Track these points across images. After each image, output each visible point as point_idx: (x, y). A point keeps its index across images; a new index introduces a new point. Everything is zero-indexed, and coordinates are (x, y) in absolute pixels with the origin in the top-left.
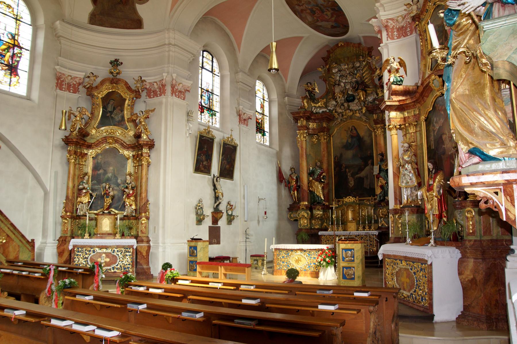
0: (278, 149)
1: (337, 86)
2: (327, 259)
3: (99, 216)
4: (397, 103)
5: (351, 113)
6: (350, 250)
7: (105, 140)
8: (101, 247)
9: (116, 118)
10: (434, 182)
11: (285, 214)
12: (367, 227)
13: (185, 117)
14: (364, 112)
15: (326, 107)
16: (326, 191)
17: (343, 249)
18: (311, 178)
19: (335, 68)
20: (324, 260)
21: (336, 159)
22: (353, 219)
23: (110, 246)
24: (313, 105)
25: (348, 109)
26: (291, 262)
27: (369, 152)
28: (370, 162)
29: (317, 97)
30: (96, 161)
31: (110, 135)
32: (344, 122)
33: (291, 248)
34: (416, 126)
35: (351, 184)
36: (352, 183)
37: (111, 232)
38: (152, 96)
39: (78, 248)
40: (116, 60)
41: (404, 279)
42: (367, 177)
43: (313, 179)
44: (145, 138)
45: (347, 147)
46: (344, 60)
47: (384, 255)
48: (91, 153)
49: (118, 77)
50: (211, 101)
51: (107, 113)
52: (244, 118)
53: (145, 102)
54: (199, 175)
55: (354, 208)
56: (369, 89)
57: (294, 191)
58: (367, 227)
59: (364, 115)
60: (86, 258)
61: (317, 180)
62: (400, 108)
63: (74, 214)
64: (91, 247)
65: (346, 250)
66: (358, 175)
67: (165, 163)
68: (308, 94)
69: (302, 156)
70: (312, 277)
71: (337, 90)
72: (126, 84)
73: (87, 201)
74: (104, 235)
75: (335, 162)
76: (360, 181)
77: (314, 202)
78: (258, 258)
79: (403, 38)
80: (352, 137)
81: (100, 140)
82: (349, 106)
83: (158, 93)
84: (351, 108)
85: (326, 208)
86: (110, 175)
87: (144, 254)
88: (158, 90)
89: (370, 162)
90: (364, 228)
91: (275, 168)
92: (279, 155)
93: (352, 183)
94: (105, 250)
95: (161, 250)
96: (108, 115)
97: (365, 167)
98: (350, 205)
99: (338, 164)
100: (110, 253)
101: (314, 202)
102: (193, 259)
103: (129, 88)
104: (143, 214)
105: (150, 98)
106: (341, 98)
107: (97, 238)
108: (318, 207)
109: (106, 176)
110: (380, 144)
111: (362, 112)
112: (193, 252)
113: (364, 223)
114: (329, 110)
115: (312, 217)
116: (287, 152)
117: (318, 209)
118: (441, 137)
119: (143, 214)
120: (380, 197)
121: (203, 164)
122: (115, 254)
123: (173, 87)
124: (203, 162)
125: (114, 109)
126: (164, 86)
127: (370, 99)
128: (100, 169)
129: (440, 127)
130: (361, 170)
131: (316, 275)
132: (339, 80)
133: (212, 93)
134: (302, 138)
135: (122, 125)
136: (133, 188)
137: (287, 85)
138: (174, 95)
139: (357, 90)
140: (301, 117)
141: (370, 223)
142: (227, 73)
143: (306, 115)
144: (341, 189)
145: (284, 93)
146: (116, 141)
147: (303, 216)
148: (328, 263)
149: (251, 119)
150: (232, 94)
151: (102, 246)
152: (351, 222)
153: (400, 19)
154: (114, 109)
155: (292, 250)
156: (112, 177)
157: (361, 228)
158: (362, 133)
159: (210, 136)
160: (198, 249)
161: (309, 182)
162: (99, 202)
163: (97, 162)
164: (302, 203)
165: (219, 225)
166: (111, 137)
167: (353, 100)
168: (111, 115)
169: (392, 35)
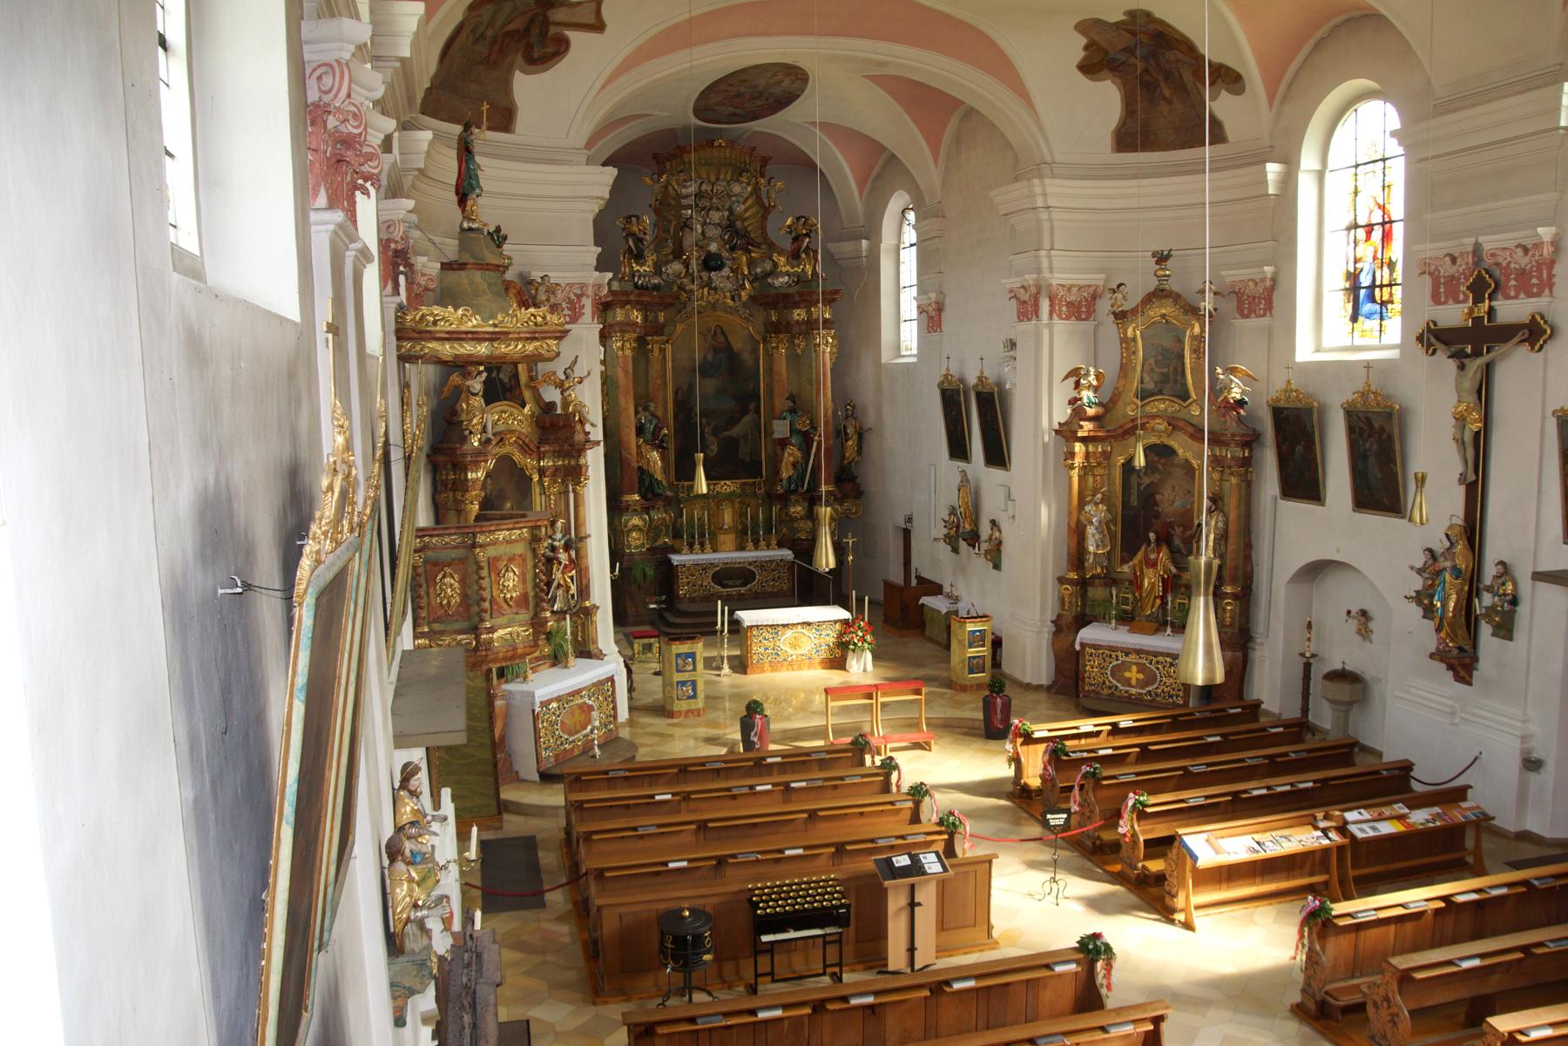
2: (868, 638)
14: (744, 298)
20: (863, 639)
22: (733, 529)
28: (752, 406)
41: (1133, 674)
45: (706, 370)
47: (1082, 645)
55: (733, 502)
59: (744, 304)
62: (1084, 440)
64: (558, 699)
71: (689, 240)
75: (676, 401)
80: (716, 350)
89: (752, 406)
99: (683, 406)
108: (660, 504)
118: (1153, 495)
130: (734, 421)
131: (837, 662)
140: (628, 302)
141: (768, 531)
152: (726, 532)
153: (1074, 290)
157: (750, 545)
158: (737, 345)
161: (638, 447)
167: (719, 268)
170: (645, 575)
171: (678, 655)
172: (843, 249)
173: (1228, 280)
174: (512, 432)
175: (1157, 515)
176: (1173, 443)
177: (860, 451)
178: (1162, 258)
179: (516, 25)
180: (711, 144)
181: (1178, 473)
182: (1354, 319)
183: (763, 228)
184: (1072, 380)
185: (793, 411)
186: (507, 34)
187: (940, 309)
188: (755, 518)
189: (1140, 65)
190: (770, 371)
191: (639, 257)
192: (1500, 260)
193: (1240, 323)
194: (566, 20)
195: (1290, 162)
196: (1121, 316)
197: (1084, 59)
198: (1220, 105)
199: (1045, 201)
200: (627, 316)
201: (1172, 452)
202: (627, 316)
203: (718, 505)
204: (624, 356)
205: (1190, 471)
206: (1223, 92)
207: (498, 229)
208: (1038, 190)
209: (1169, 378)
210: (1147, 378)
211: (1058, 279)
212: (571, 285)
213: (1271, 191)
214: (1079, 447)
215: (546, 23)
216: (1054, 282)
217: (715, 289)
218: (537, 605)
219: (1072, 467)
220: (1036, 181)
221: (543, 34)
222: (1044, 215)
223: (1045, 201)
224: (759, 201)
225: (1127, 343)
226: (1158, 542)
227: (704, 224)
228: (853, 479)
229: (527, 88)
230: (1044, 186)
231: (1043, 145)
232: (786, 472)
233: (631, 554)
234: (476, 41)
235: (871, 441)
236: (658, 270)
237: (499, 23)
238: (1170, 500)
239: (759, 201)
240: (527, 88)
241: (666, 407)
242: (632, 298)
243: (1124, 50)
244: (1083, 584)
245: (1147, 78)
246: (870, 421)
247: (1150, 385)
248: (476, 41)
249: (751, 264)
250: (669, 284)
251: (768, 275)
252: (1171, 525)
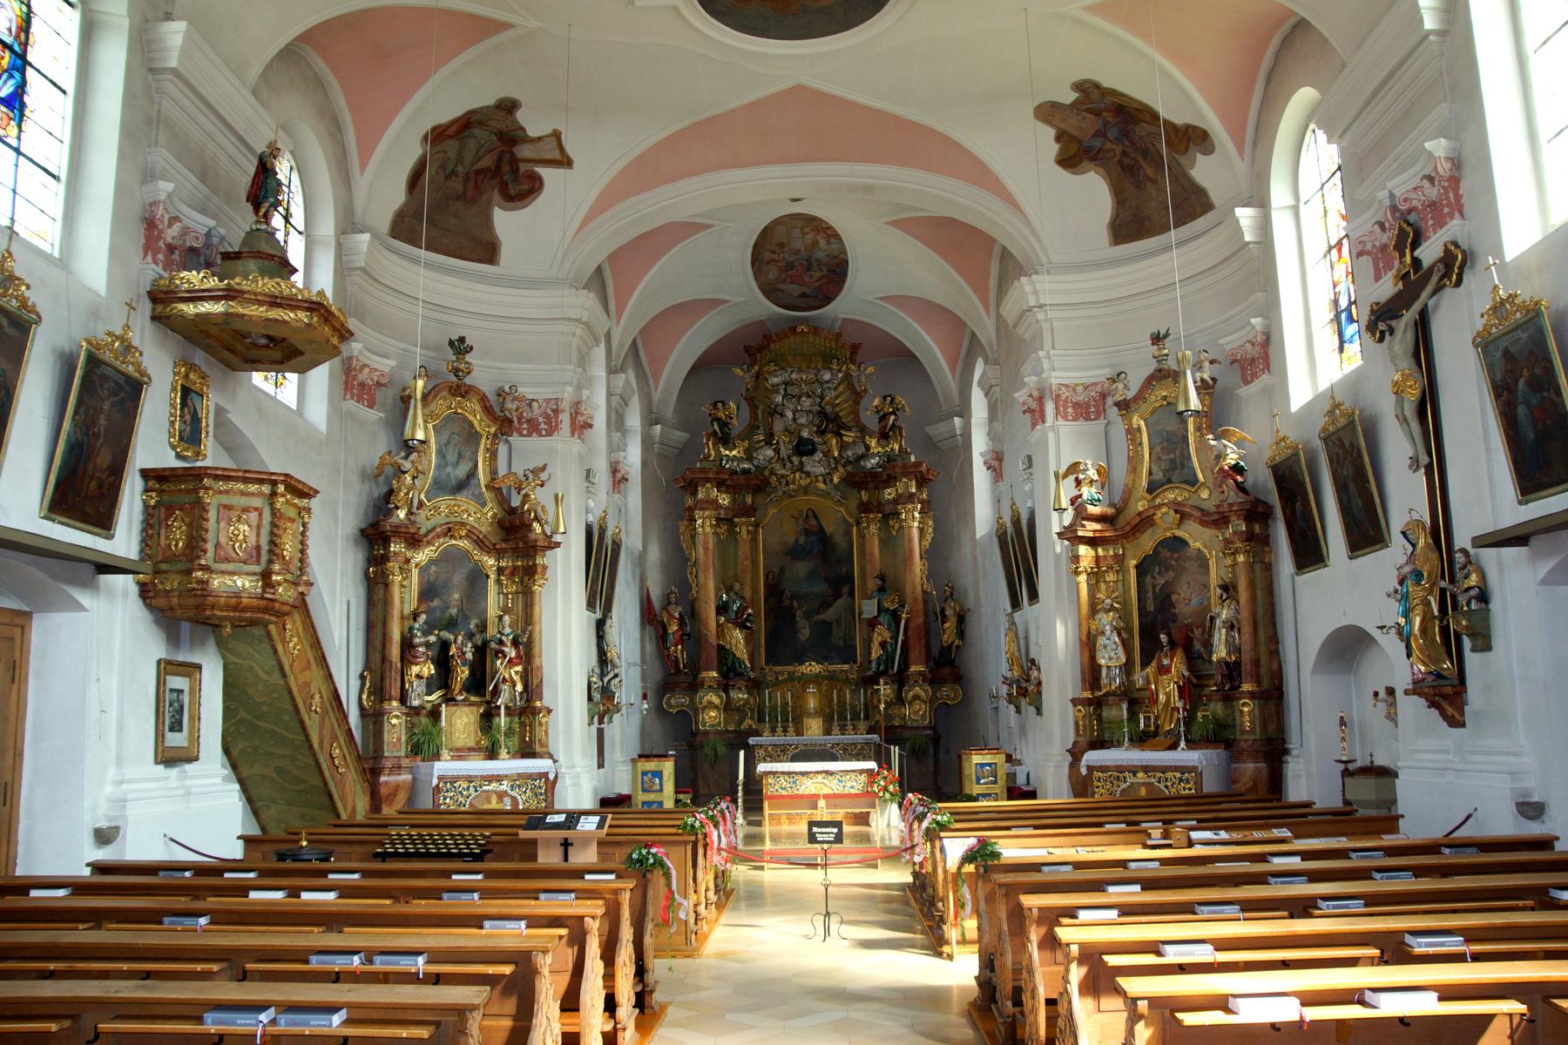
2: (891, 788)
4: (1091, 534)
12: (780, 729)
14: (836, 480)
15: (749, 458)
19: (773, 374)
20: (885, 789)
29: (734, 433)
36: (805, 632)
40: (462, 340)
42: (838, 622)
43: (727, 621)
45: (795, 553)
49: (468, 381)
55: (818, 685)
58: (780, 729)
59: (836, 487)
62: (1092, 542)
64: (470, 779)
65: (983, 765)
66: (821, 617)
69: (706, 570)
71: (778, 426)
74: (460, 754)
75: (767, 585)
76: (824, 629)
79: (1081, 422)
80: (807, 532)
82: (801, 463)
83: (543, 426)
85: (755, 686)
86: (454, 611)
89: (845, 590)
90: (785, 731)
94: (494, 786)
98: (811, 681)
99: (774, 589)
108: (741, 683)
110: (872, 554)
115: (728, 707)
116: (655, 554)
118: (1168, 596)
120: (879, 665)
130: (826, 604)
136: (515, 643)
137: (656, 396)
140: (708, 480)
141: (855, 716)
145: (650, 418)
147: (710, 703)
152: (810, 715)
153: (1080, 389)
155: (804, 774)
157: (836, 729)
158: (829, 528)
160: (665, 777)
161: (719, 626)
164: (704, 674)
167: (811, 452)
169: (1066, 413)
170: (716, 754)
171: (644, 773)
172: (937, 430)
173: (1228, 348)
174: (463, 524)
175: (1174, 618)
176: (1179, 533)
177: (961, 634)
178: (1157, 339)
179: (487, 162)
180: (793, 330)
181: (1192, 566)
182: (1341, 349)
183: (856, 413)
184: (1072, 478)
185: (881, 590)
186: (478, 172)
187: (999, 459)
188: (842, 703)
189: (1118, 149)
190: (863, 553)
191: (725, 440)
192: (1415, 203)
193: (1244, 391)
194: (533, 156)
195: (1261, 201)
196: (1124, 406)
197: (1061, 151)
198: (1203, 170)
199: (1037, 299)
200: (708, 493)
201: (1184, 543)
202: (708, 493)
203: (805, 687)
204: (704, 533)
205: (1203, 563)
206: (1199, 156)
207: (462, 340)
208: (1028, 288)
209: (1174, 465)
210: (1155, 469)
211: (1056, 378)
212: (548, 401)
213: (1247, 238)
214: (1083, 550)
215: (515, 162)
216: (1054, 382)
217: (808, 474)
218: (270, 561)
219: (1076, 573)
220: (1024, 279)
221: (515, 171)
222: (1041, 316)
223: (1037, 299)
224: (851, 386)
225: (1132, 433)
226: (1173, 644)
227: (795, 412)
228: (951, 663)
229: (506, 222)
230: (1032, 283)
231: (1036, 246)
232: (876, 652)
233: (706, 733)
234: (448, 177)
235: (972, 626)
236: (749, 458)
237: (469, 157)
238: (1186, 601)
239: (851, 386)
240: (506, 222)
243: (1097, 134)
244: (1097, 703)
245: (1127, 161)
246: (970, 603)
247: (1159, 476)
248: (448, 177)
249: (843, 446)
250: (760, 469)
251: (863, 457)
252: (1189, 628)
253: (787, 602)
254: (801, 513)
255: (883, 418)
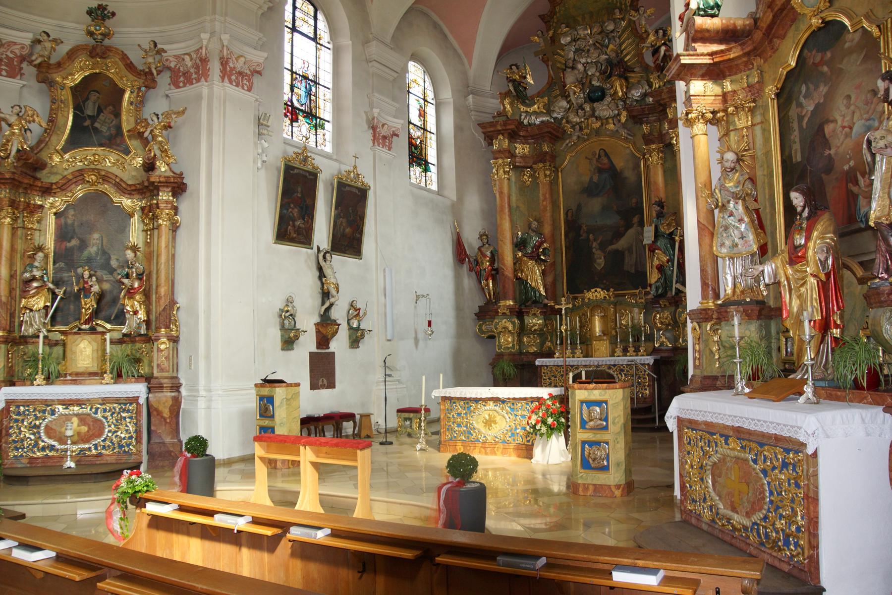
0: (454, 198)
1: (569, 70)
2: (550, 421)
3: (70, 337)
4: (707, 60)
5: (598, 124)
6: (599, 403)
7: (79, 176)
8: (67, 403)
9: (104, 129)
10: (808, 239)
11: (471, 325)
12: (631, 349)
13: (252, 128)
14: (623, 120)
15: (549, 112)
16: (550, 279)
17: (582, 402)
18: (520, 254)
19: (565, 34)
20: (544, 422)
21: (570, 214)
22: (604, 333)
23: (88, 400)
24: (523, 108)
25: (593, 115)
26: (475, 425)
27: (634, 201)
28: (636, 220)
29: (530, 93)
30: (63, 220)
31: (92, 166)
32: (585, 141)
33: (473, 396)
34: (752, 110)
35: (599, 264)
36: (600, 262)
37: (95, 369)
38: (181, 84)
39: (18, 407)
42: (630, 249)
43: (524, 255)
44: (163, 169)
45: (590, 190)
46: (584, 18)
47: (680, 421)
48: (54, 203)
49: (107, 42)
50: (313, 98)
51: (84, 119)
52: (383, 133)
53: (167, 96)
54: (286, 249)
55: (605, 310)
56: (633, 75)
57: (487, 280)
58: (631, 349)
59: (624, 126)
60: (36, 427)
61: (531, 258)
62: (714, 72)
63: (16, 334)
64: (47, 403)
65: (590, 403)
67: (209, 223)
68: (512, 88)
70: (519, 456)
71: (570, 78)
72: (124, 57)
73: (41, 305)
74: (79, 377)
76: (616, 259)
77: (527, 300)
78: (412, 415)
80: (600, 171)
81: (70, 177)
82: (593, 110)
83: (194, 76)
84: (597, 114)
85: (550, 313)
87: (166, 413)
88: (192, 70)
89: (636, 220)
90: (625, 351)
91: (449, 234)
92: (456, 210)
93: (600, 262)
94: (76, 409)
95: (202, 404)
96: (87, 123)
97: (626, 230)
99: (573, 225)
100: (89, 415)
101: (527, 300)
102: (266, 423)
103: (130, 67)
104: (163, 331)
105: (178, 87)
106: (577, 95)
107: (65, 382)
108: (534, 310)
109: (86, 253)
110: (655, 183)
111: (619, 121)
112: (267, 409)
113: (625, 340)
114: (555, 119)
115: (523, 330)
116: (473, 203)
117: (534, 314)
118: (821, 129)
119: (163, 331)
120: (657, 289)
121: (294, 226)
122: (99, 416)
123: (224, 62)
124: (294, 221)
125: (100, 111)
126: (204, 61)
127: (636, 94)
128: (72, 238)
129: (817, 106)
130: (618, 235)
131: (527, 451)
132: (574, 60)
133: (316, 83)
134: (501, 173)
135: (118, 145)
136: (140, 277)
137: (471, 73)
138: (226, 79)
139: (610, 76)
140: (499, 132)
141: (637, 340)
142: (346, 41)
143: (508, 127)
144: (580, 276)
145: (465, 89)
146: (105, 178)
147: (505, 328)
148: (551, 429)
149: (397, 135)
150: (355, 84)
151: (70, 400)
152: (599, 339)
154: (100, 111)
155: (477, 400)
156: (97, 254)
157: (619, 351)
158: (619, 163)
159: (309, 168)
160: (277, 402)
161: (517, 261)
162: (72, 307)
163: (66, 223)
164: (502, 303)
165: (331, 350)
166: (93, 170)
168: (93, 124)
185: (660, 215)
241: (554, 225)
242: (499, 128)
253: (584, 236)
254: (594, 154)
255: (656, 51)
